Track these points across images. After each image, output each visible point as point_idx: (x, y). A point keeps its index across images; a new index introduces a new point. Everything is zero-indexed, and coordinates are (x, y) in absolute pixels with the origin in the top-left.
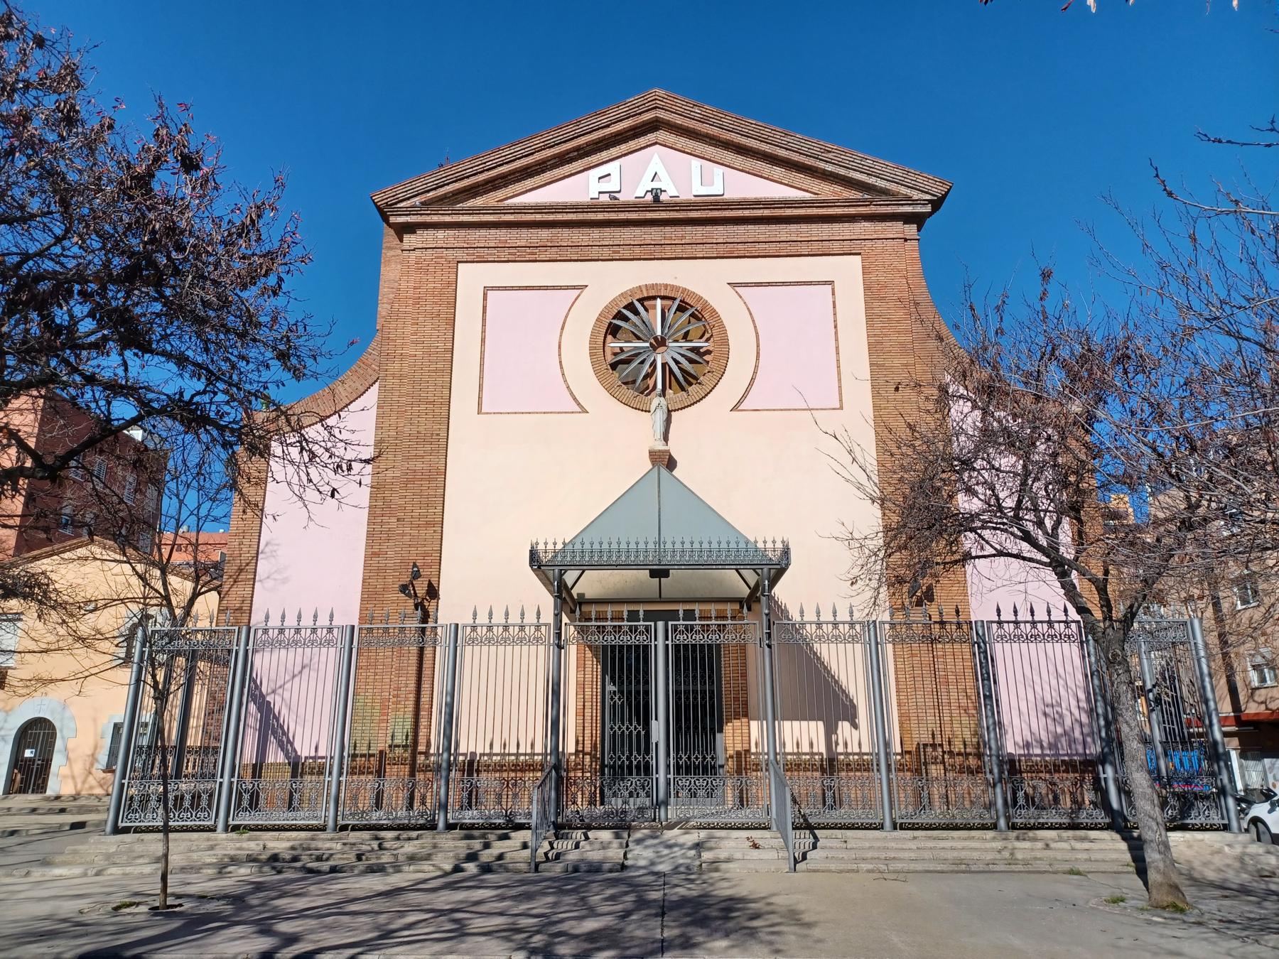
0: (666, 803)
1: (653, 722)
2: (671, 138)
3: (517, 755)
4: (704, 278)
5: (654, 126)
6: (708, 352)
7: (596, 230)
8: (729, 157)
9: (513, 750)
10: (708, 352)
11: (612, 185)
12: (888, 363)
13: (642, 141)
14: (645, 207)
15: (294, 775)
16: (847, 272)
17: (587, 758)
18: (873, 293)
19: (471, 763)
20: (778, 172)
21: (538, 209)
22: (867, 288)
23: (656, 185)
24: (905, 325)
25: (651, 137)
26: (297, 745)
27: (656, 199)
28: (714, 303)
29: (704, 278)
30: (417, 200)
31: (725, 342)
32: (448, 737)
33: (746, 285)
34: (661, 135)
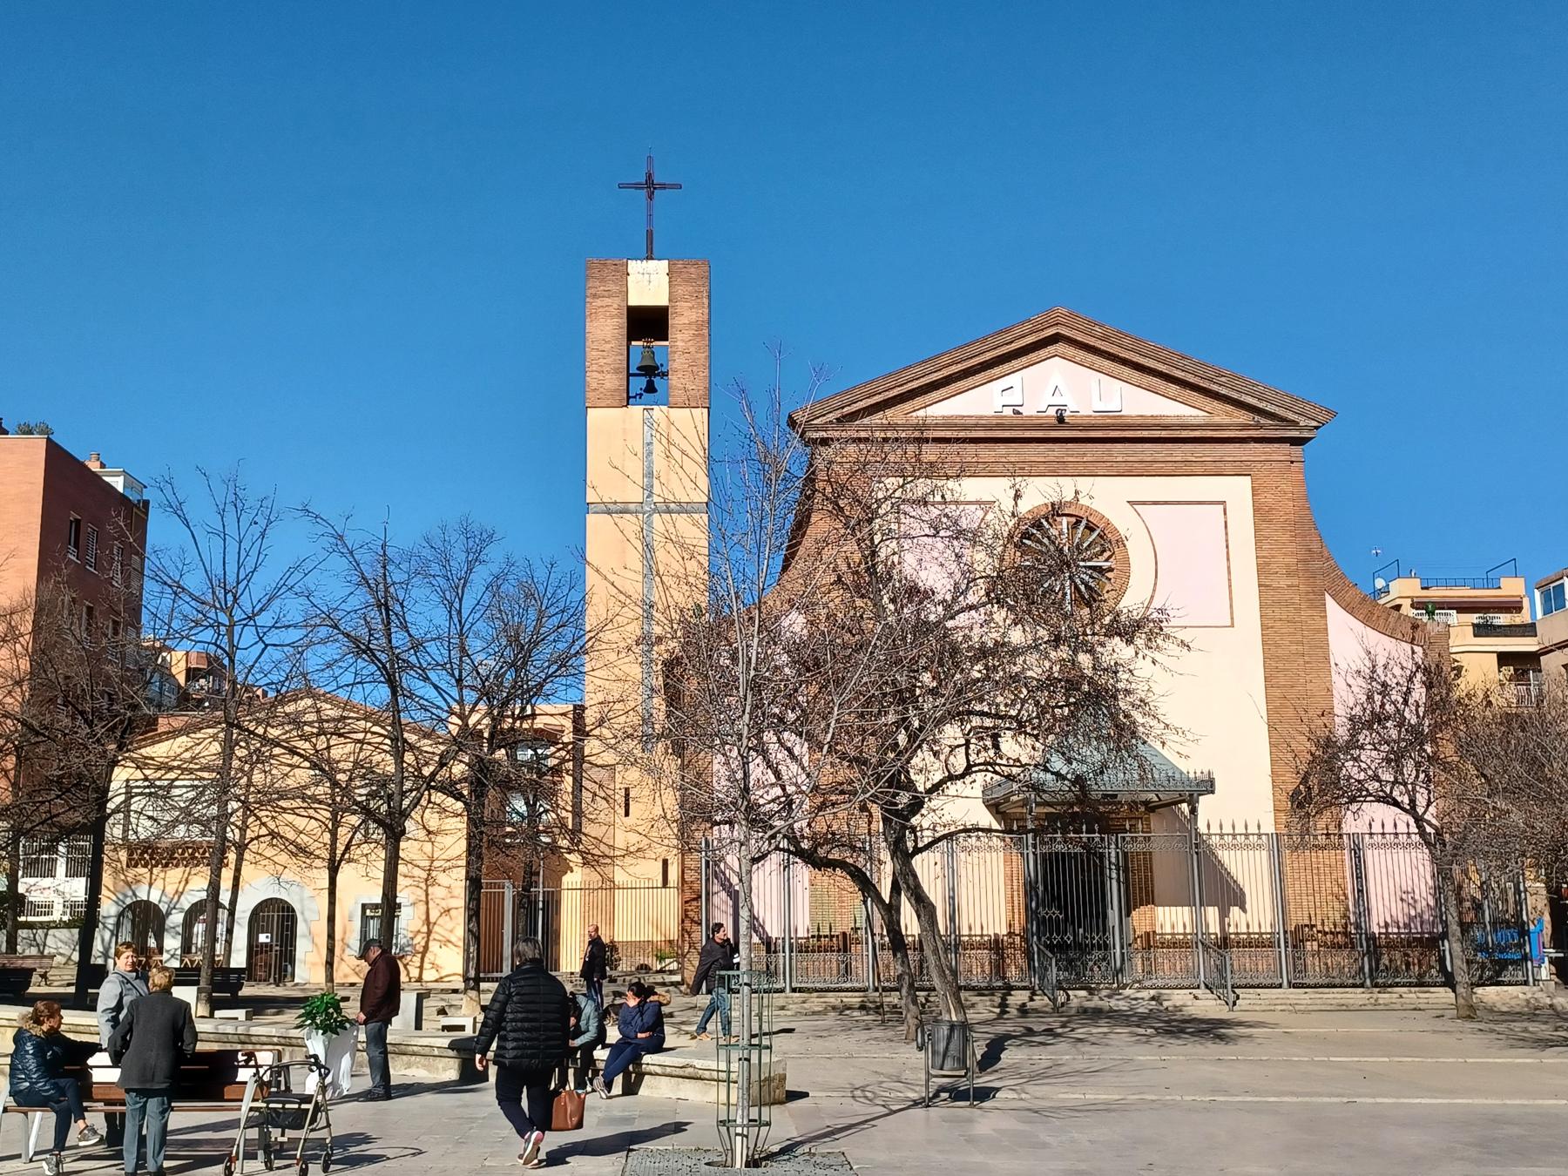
0: (1121, 970)
1: (1110, 911)
2: (1071, 351)
3: (1185, 934)
4: (1107, 496)
5: (1055, 339)
6: (1111, 570)
7: (1002, 446)
8: (1127, 371)
9: (1244, 930)
10: (1111, 570)
11: (1014, 398)
12: (1275, 584)
13: (1043, 353)
14: (1051, 428)
15: (768, 951)
16: (1237, 490)
17: (1018, 939)
18: (1262, 513)
19: (996, 941)
20: (1173, 389)
21: (948, 423)
22: (1256, 510)
23: (1057, 400)
24: (1292, 547)
25: (1051, 349)
26: (768, 929)
27: (1061, 419)
28: (1116, 522)
29: (1107, 496)
30: (831, 417)
31: (1126, 561)
32: (952, 919)
33: (1144, 503)
34: (1060, 347)
